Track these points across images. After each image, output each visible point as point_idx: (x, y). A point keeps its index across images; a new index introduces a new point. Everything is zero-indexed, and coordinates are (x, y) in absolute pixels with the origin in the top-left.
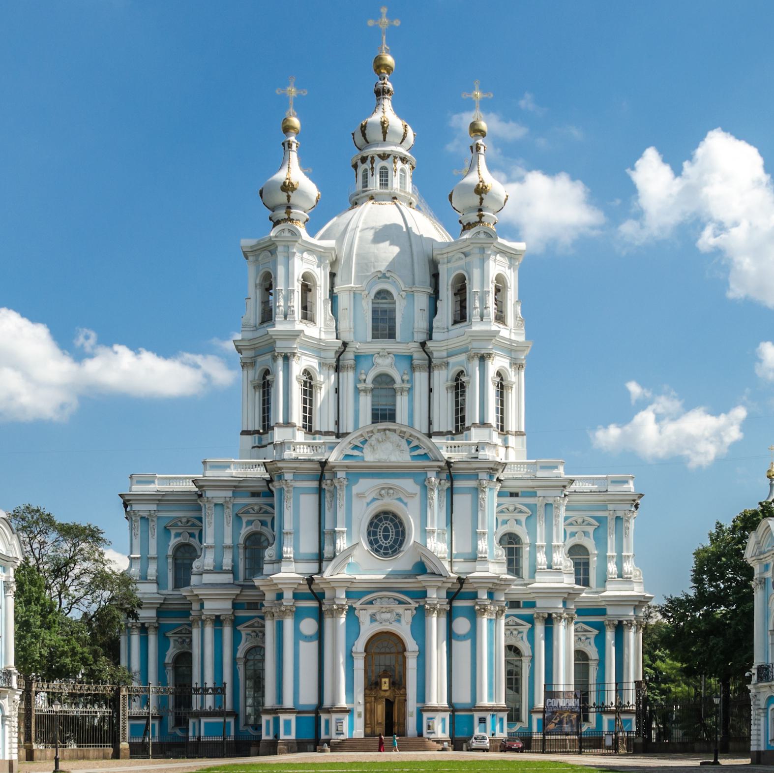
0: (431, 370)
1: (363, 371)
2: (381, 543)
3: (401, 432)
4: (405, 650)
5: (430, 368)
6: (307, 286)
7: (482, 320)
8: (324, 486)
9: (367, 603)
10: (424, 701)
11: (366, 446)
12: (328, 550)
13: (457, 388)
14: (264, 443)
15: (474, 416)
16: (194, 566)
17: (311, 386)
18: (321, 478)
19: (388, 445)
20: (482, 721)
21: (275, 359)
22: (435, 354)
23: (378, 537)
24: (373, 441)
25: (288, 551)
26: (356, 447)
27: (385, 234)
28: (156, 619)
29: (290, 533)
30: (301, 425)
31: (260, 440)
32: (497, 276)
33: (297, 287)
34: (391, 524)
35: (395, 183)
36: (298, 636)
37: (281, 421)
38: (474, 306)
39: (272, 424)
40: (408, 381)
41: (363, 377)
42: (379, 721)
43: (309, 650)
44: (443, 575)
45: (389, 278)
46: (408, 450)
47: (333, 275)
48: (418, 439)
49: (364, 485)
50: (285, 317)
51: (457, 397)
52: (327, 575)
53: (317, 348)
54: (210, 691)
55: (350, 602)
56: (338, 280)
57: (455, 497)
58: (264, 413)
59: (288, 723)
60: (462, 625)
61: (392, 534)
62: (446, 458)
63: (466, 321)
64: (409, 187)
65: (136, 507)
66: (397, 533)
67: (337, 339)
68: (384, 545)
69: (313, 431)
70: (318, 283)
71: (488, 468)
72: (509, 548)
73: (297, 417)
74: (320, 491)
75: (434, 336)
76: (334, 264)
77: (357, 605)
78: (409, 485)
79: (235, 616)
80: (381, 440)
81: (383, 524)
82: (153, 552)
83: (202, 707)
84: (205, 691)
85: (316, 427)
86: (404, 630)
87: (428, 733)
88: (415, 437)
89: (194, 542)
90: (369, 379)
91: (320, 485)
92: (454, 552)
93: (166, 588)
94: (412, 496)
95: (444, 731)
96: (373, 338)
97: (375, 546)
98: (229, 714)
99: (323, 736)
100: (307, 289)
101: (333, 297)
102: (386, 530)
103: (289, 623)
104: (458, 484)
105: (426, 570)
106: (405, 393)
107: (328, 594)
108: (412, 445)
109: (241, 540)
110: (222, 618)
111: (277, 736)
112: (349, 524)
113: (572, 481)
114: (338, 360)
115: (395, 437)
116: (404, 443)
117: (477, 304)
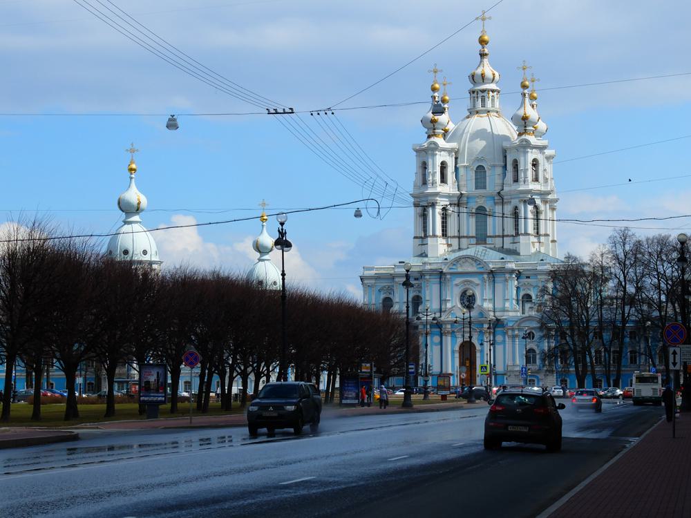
5: (503, 204)
15: (521, 231)
19: (467, 264)
22: (505, 197)
24: (461, 262)
26: (454, 265)
27: (481, 134)
31: (422, 242)
33: (438, 170)
37: (431, 234)
38: (522, 175)
43: (436, 349)
47: (456, 158)
49: (458, 280)
50: (433, 185)
52: (442, 318)
53: (448, 196)
56: (459, 160)
60: (499, 338)
65: (366, 282)
70: (449, 165)
74: (440, 283)
75: (506, 188)
76: (456, 153)
77: (456, 330)
78: (476, 280)
85: (449, 234)
89: (391, 296)
101: (456, 169)
104: (496, 279)
109: (410, 299)
112: (452, 297)
114: (459, 201)
117: (522, 174)
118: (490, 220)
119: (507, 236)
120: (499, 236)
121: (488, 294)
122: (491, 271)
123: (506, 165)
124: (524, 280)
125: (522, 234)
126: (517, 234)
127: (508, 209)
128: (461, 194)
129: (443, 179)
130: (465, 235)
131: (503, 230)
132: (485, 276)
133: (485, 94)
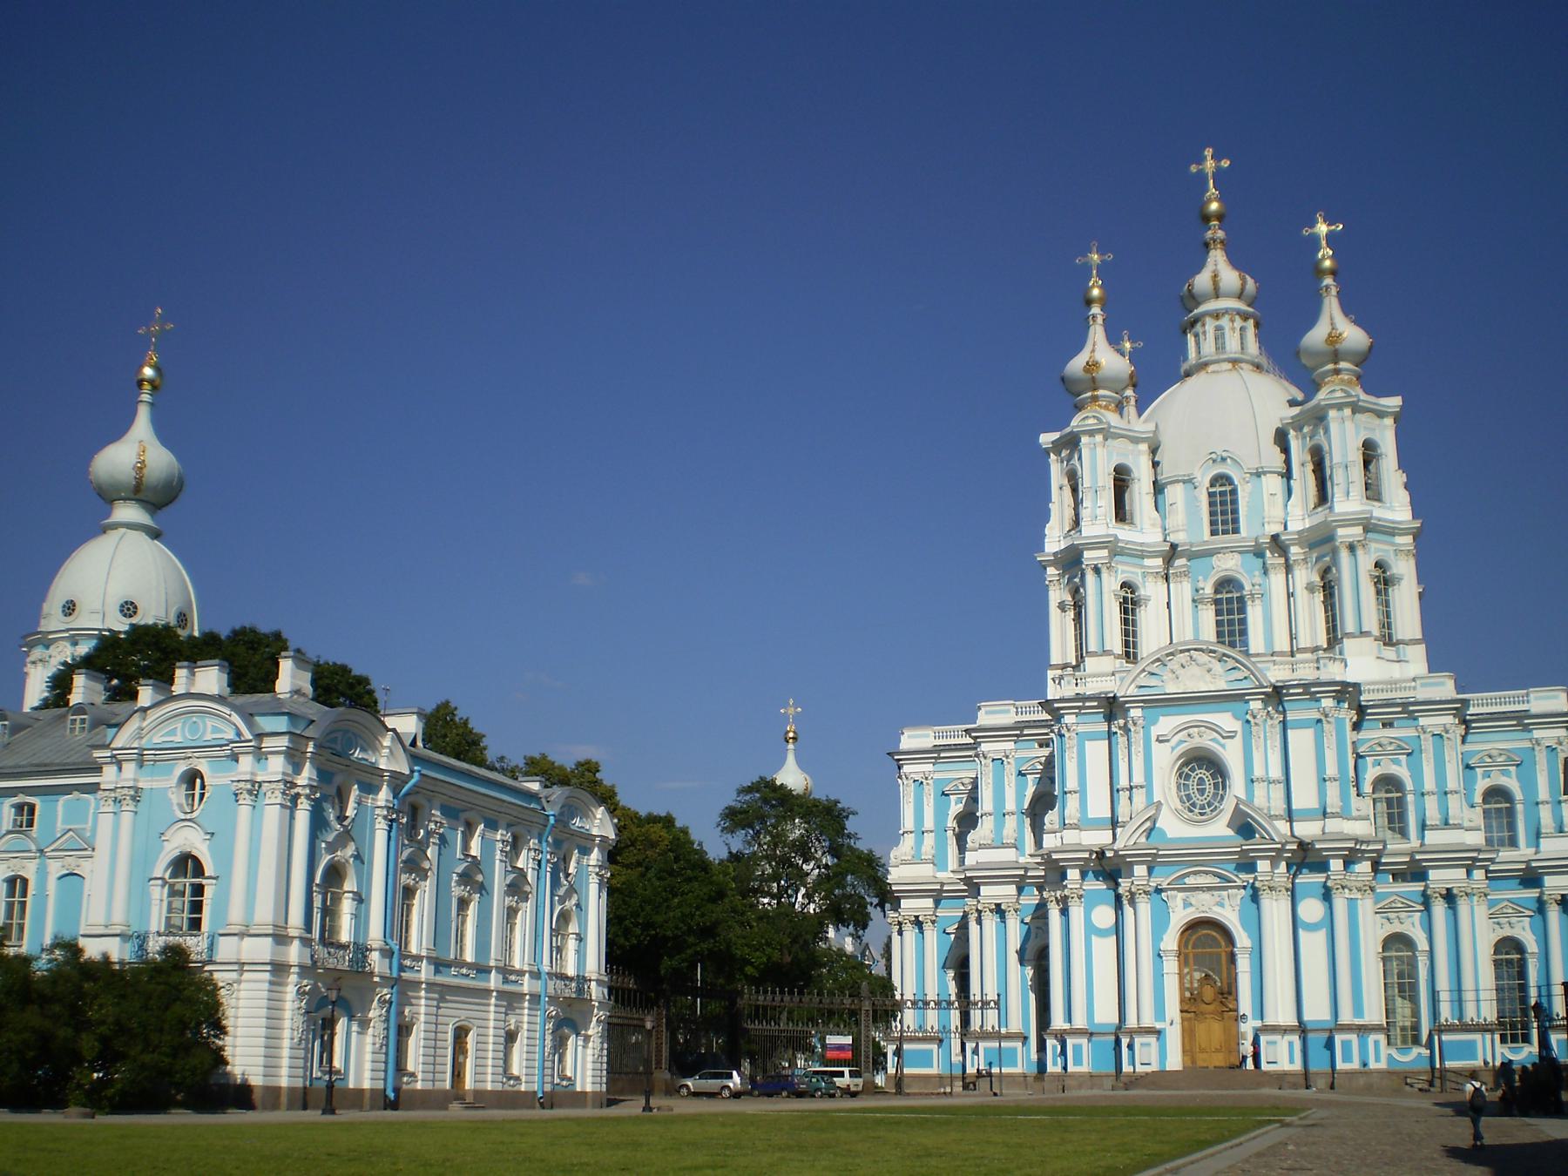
1: (1200, 578)
3: (1212, 651)
5: (1288, 569)
6: (1124, 480)
8: (1114, 729)
12: (1123, 812)
16: (968, 840)
17: (1134, 603)
19: (1194, 669)
20: (1346, 1046)
24: (1174, 664)
29: (1075, 792)
32: (1365, 440)
34: (1208, 774)
35: (1232, 344)
36: (1091, 930)
40: (1260, 585)
41: (1201, 585)
42: (1203, 1046)
43: (1105, 949)
44: (1277, 840)
47: (1155, 464)
48: (1234, 658)
49: (1167, 723)
52: (1119, 845)
54: (992, 1004)
57: (1290, 732)
59: (1077, 1048)
62: (1273, 681)
64: (1253, 347)
66: (1216, 786)
67: (1165, 541)
70: (1135, 474)
71: (1334, 691)
72: (1387, 798)
73: (1115, 643)
74: (1110, 735)
75: (1290, 528)
78: (1225, 720)
80: (1185, 664)
81: (1197, 774)
82: (929, 823)
83: (982, 1026)
84: (985, 1004)
86: (1229, 915)
87: (1268, 1063)
88: (1229, 657)
90: (1209, 590)
91: (1109, 728)
92: (1294, 807)
93: (945, 870)
94: (1231, 736)
95: (1291, 1061)
96: (1212, 535)
98: (1009, 1037)
99: (1126, 1068)
100: (1121, 481)
103: (1076, 912)
110: (1003, 907)
111: (1065, 1068)
113: (1465, 703)
115: (1203, 658)
116: (1218, 667)
118: (1254, 614)
119: (1304, 650)
122: (1275, 688)
123: (1287, 475)
124: (1373, 734)
125: (1350, 635)
126: (1334, 637)
127: (1305, 575)
128: (1174, 547)
129: (1121, 514)
131: (1292, 637)
132: (1256, 705)
133: (1225, 322)
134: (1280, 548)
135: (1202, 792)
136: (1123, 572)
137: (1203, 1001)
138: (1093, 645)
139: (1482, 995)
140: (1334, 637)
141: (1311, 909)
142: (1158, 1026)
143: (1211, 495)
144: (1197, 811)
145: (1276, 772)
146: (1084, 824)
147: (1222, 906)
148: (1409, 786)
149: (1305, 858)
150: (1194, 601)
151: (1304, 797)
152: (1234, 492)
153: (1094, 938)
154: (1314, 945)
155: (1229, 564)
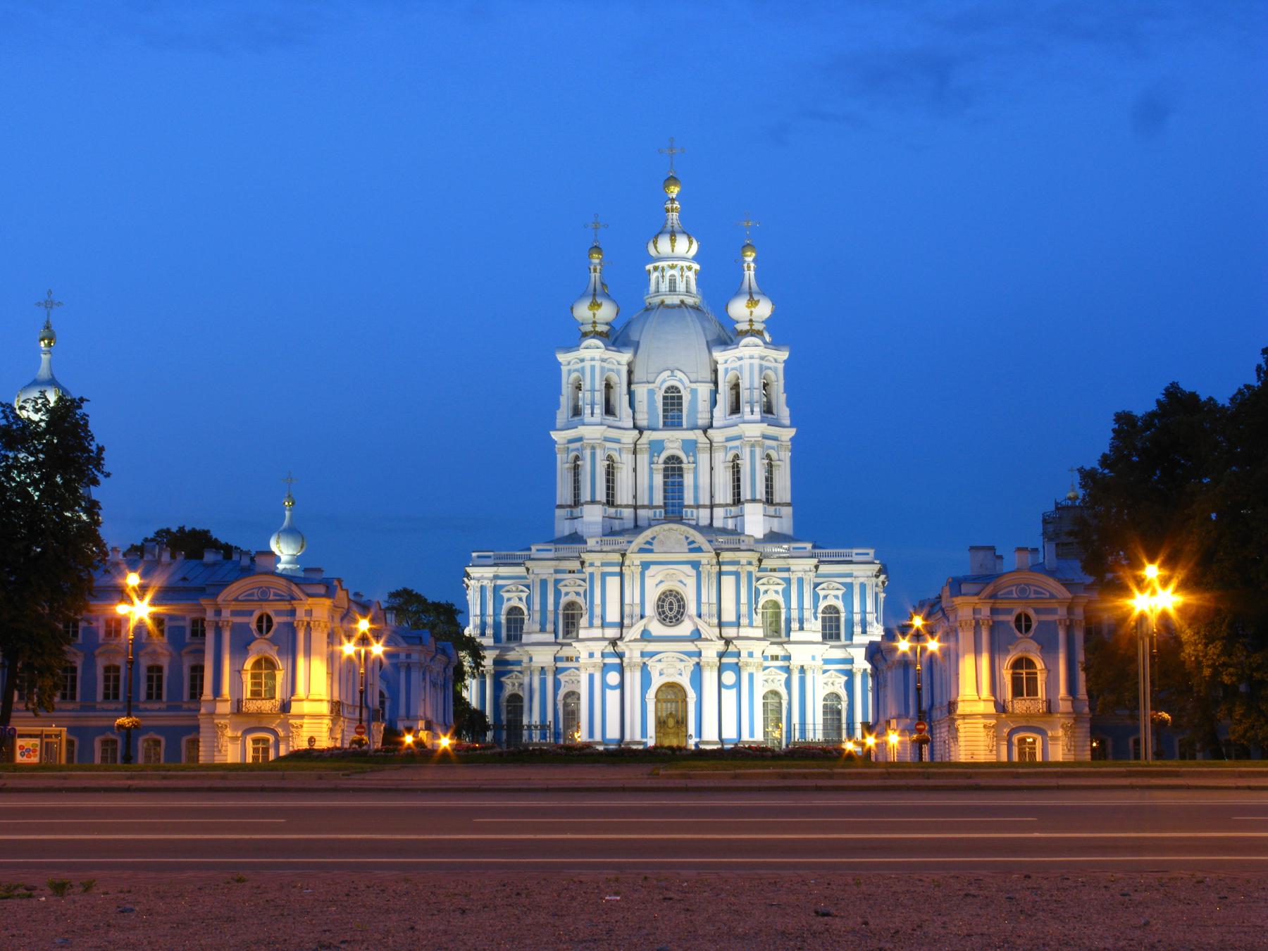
0: (713, 452)
1: (656, 454)
2: (667, 613)
4: (686, 697)
7: (752, 414)
8: (624, 571)
9: (657, 661)
10: (700, 737)
11: (656, 540)
12: (626, 621)
13: (733, 467)
14: (575, 515)
17: (613, 468)
18: (622, 564)
21: (583, 448)
23: (665, 609)
25: (597, 622)
28: (493, 667)
30: (605, 501)
31: (572, 512)
36: (605, 686)
37: (588, 499)
39: (582, 500)
41: (655, 459)
43: (613, 697)
45: (676, 377)
46: (686, 544)
47: (630, 372)
51: (734, 475)
52: (627, 639)
54: (539, 727)
55: (645, 660)
58: (575, 490)
60: (729, 678)
61: (675, 607)
63: (739, 412)
66: (679, 607)
68: (669, 615)
69: (615, 504)
73: (601, 495)
79: (557, 668)
82: (490, 610)
86: (685, 681)
91: (621, 570)
97: (663, 616)
102: (671, 604)
105: (700, 635)
106: (692, 471)
107: (627, 655)
108: (689, 540)
114: (635, 444)
119: (720, 506)
120: (704, 506)
121: (709, 595)
126: (737, 501)
127: (721, 459)
129: (609, 410)
130: (646, 503)
131: (712, 497)
134: (707, 438)
135: (671, 610)
136: (608, 449)
137: (668, 727)
138: (586, 495)
139: (817, 727)
140: (737, 501)
141: (729, 678)
142: (644, 740)
143: (665, 398)
144: (668, 620)
145: (714, 600)
146: (604, 625)
147: (681, 674)
148: (782, 605)
149: (728, 649)
150: (651, 469)
151: (729, 615)
152: (680, 398)
153: (608, 692)
154: (729, 696)
155: (673, 449)
